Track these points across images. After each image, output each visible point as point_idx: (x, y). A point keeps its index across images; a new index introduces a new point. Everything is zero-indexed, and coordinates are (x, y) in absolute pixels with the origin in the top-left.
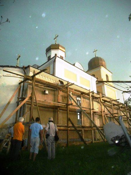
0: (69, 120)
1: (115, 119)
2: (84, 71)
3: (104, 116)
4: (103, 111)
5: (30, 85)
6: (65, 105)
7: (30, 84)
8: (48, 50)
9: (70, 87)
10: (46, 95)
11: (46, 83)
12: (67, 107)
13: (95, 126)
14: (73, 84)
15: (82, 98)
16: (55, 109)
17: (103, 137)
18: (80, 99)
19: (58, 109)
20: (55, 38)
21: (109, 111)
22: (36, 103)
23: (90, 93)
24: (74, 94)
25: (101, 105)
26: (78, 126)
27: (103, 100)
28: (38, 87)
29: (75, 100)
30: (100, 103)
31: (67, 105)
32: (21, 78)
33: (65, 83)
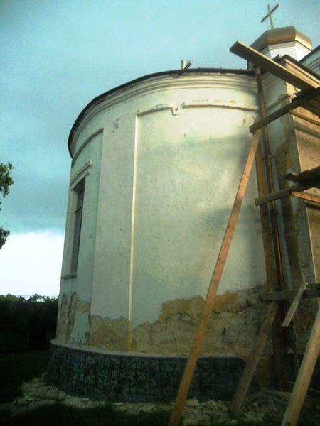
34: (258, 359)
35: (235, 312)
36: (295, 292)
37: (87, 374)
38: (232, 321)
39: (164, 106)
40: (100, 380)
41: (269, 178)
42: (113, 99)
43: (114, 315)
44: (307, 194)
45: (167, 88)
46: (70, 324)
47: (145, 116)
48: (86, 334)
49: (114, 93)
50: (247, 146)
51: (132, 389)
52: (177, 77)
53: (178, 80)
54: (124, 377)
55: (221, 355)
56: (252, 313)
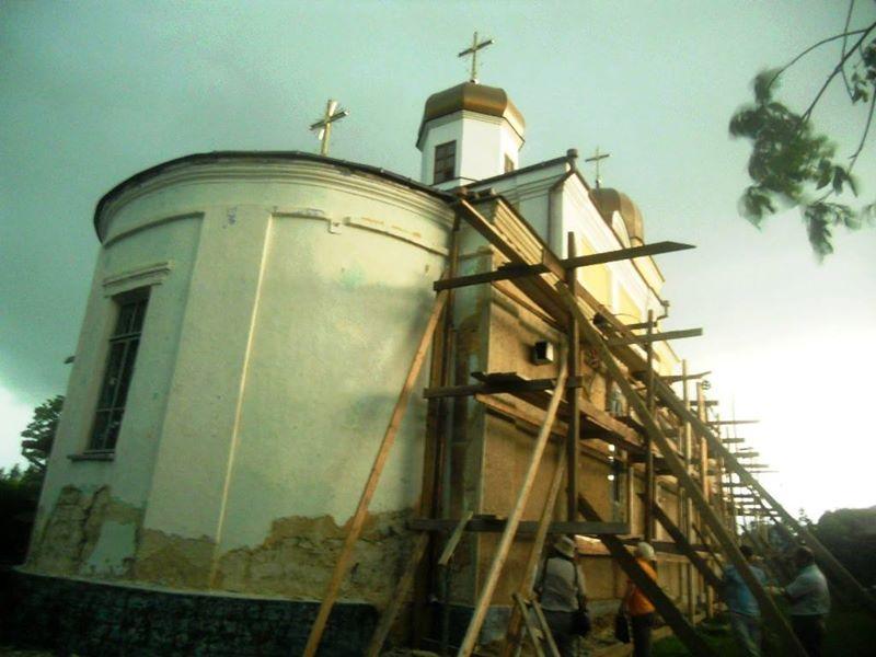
8: (445, 107)
34: (397, 606)
35: (371, 541)
36: (455, 523)
37: (126, 625)
38: (369, 555)
39: (320, 215)
40: (155, 635)
41: (445, 360)
42: (231, 168)
43: (191, 530)
44: (497, 399)
45: (329, 185)
46: (84, 541)
47: (285, 220)
48: (126, 560)
49: (234, 160)
50: (424, 307)
51: (212, 647)
52: (346, 174)
53: (348, 178)
54: (202, 628)
55: (348, 601)
56: (393, 544)
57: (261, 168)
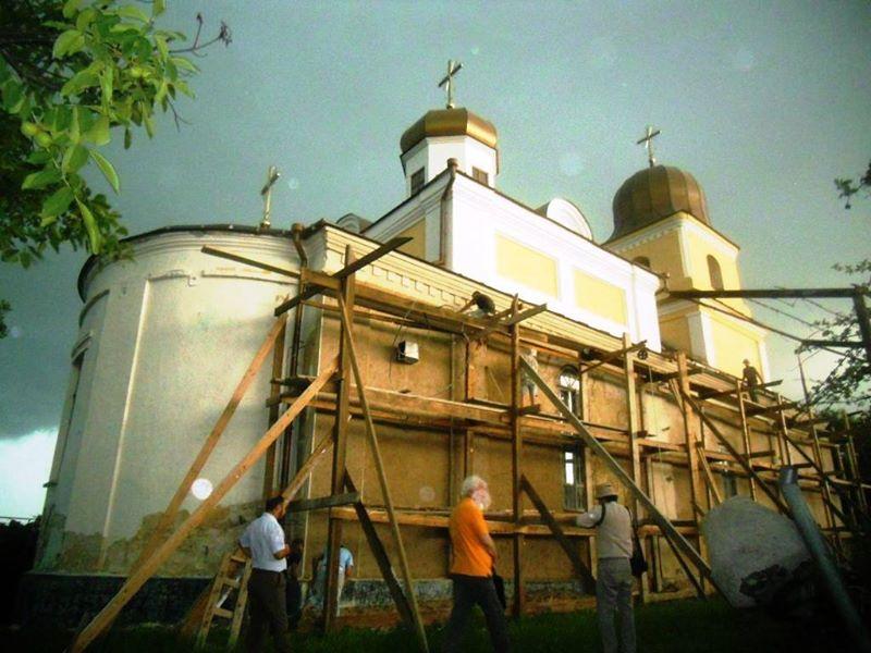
0: (522, 486)
1: (758, 481)
2: (592, 242)
3: (701, 468)
4: (692, 441)
5: (326, 316)
6: (501, 416)
7: (330, 313)
8: (414, 140)
9: (524, 323)
10: (407, 368)
11: (404, 306)
12: (512, 425)
13: (655, 517)
14: (542, 308)
15: (585, 376)
16: (450, 434)
17: (695, 572)
18: (576, 385)
19: (469, 433)
20: (447, 79)
21: (723, 442)
22: (361, 404)
23: (625, 351)
24: (544, 359)
25: (684, 414)
26: (570, 515)
27: (693, 387)
28: (367, 329)
29: (550, 385)
30: (680, 402)
31: (514, 412)
32: (286, 284)
33: (501, 305)
39: (180, 273)
43: (89, 532)
57: (143, 245)
